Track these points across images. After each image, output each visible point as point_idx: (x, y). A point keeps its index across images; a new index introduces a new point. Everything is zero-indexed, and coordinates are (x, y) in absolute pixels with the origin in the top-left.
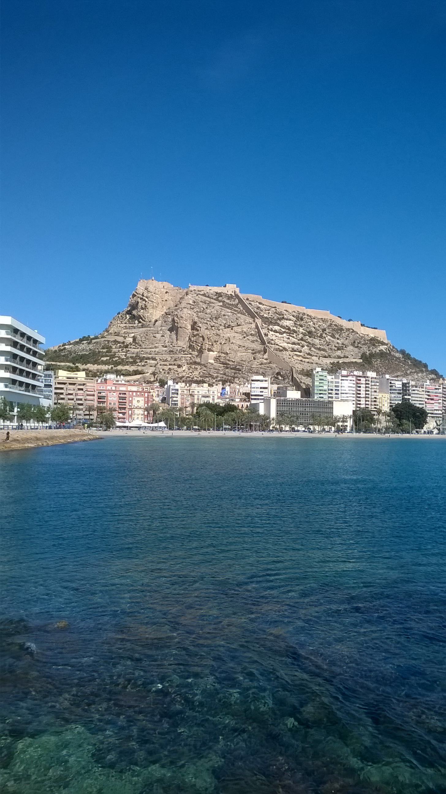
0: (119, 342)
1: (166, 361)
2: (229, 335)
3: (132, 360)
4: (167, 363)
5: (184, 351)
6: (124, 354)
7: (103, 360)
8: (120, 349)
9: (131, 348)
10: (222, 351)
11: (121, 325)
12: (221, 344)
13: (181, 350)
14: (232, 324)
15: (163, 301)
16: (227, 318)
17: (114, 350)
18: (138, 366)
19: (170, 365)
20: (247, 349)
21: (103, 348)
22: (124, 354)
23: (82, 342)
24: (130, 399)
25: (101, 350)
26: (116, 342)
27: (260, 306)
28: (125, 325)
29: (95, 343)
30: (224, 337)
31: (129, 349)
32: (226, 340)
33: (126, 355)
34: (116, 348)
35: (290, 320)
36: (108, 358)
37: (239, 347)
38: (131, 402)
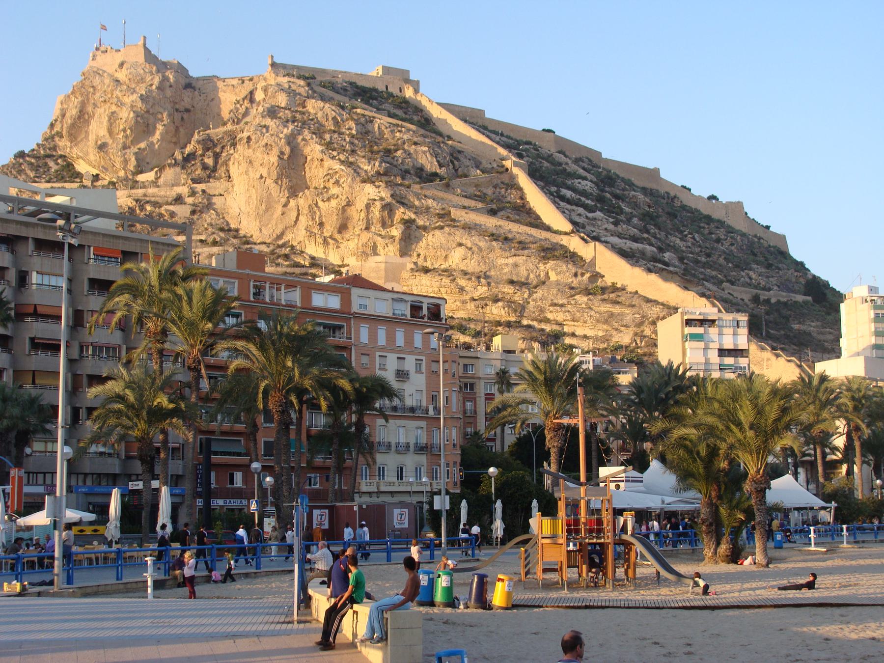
5: (286, 257)
13: (273, 253)
14: (442, 171)
16: (424, 152)
28: (49, 185)
35: (585, 178)
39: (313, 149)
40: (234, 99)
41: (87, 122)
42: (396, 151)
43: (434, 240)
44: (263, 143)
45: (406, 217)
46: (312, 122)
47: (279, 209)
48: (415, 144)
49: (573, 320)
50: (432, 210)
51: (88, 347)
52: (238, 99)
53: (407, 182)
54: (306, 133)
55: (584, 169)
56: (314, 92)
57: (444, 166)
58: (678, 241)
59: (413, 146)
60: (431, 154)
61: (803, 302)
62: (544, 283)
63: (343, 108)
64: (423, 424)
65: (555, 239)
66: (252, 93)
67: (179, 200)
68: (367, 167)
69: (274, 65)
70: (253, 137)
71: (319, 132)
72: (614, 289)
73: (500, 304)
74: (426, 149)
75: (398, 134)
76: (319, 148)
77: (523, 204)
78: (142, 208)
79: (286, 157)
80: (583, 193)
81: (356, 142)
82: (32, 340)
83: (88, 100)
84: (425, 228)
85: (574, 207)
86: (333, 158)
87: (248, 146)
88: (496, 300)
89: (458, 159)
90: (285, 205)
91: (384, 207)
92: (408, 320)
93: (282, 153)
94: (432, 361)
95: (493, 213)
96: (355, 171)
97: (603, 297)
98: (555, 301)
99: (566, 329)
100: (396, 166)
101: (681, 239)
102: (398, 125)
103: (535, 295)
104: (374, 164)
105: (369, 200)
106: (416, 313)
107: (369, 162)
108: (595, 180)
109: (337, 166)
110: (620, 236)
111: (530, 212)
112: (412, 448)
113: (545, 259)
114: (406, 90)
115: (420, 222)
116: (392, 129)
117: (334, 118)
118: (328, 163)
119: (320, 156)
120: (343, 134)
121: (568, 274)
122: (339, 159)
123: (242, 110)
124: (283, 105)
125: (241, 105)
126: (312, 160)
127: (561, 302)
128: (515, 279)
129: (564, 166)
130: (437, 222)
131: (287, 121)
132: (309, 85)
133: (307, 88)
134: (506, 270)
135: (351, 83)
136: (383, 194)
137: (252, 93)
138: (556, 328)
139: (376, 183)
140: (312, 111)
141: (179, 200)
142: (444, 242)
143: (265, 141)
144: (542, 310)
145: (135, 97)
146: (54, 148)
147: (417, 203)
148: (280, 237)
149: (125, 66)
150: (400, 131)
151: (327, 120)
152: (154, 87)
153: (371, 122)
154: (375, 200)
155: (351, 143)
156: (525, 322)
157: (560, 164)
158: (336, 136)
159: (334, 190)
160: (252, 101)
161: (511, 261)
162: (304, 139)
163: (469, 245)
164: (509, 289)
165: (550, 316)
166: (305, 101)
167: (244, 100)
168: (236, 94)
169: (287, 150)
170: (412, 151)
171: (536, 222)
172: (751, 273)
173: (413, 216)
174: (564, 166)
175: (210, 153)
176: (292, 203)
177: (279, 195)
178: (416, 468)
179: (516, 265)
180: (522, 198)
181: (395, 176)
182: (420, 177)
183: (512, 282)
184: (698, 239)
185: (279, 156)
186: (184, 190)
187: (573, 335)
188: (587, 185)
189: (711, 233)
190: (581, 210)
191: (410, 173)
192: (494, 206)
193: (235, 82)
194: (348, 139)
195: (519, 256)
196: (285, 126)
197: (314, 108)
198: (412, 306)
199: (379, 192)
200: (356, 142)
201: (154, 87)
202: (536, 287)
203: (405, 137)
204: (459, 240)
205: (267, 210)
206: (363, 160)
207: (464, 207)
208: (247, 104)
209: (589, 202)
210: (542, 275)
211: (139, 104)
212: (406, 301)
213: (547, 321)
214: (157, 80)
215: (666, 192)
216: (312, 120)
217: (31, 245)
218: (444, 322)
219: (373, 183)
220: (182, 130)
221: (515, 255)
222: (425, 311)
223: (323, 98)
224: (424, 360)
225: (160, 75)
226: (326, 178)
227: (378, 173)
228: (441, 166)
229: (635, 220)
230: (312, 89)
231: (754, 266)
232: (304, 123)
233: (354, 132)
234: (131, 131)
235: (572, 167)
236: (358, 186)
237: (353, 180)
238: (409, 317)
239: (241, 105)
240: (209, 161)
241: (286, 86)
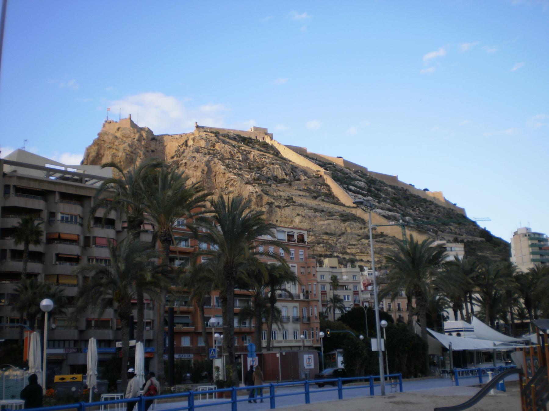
2: (288, 193)
10: (284, 219)
12: (279, 207)
14: (287, 178)
15: (148, 151)
16: (277, 168)
20: (330, 214)
32: (287, 200)
35: (360, 181)
37: (315, 212)
39: (220, 168)
40: (177, 145)
42: (263, 168)
43: (285, 213)
44: (193, 166)
45: (270, 201)
46: (219, 154)
48: (273, 164)
49: (361, 253)
50: (282, 197)
51: (93, 259)
52: (179, 145)
53: (269, 183)
54: (216, 160)
55: (359, 176)
56: (219, 139)
57: (288, 175)
58: (411, 212)
59: (272, 165)
60: (281, 169)
61: (481, 241)
62: (343, 233)
63: (234, 147)
64: (297, 304)
65: (348, 211)
66: (186, 141)
68: (249, 177)
69: (198, 127)
70: (188, 163)
71: (222, 159)
73: (322, 245)
74: (278, 166)
75: (264, 159)
76: (223, 167)
77: (330, 193)
79: (205, 172)
80: (360, 188)
81: (242, 164)
82: (57, 255)
83: (101, 147)
84: (279, 207)
85: (357, 195)
86: (230, 172)
87: (186, 167)
88: (319, 244)
89: (295, 172)
91: (258, 196)
92: (286, 243)
93: (203, 170)
94: (301, 267)
95: (315, 198)
96: (242, 178)
97: (376, 240)
98: (351, 243)
99: (358, 258)
100: (263, 176)
101: (413, 210)
102: (263, 155)
103: (340, 240)
104: (252, 175)
105: (250, 193)
106: (290, 239)
107: (249, 174)
108: (366, 181)
109: (233, 176)
110: (382, 209)
111: (334, 197)
112: (291, 319)
113: (344, 221)
114: (266, 138)
115: (276, 204)
116: (260, 157)
117: (230, 152)
118: (228, 175)
119: (223, 171)
120: (235, 160)
121: (357, 228)
122: (233, 173)
123: (182, 150)
124: (203, 146)
125: (181, 148)
126: (219, 173)
127: (354, 243)
128: (329, 232)
129: (349, 175)
130: (286, 204)
131: (206, 154)
132: (216, 136)
133: (215, 138)
134: (324, 227)
135: (238, 135)
136: (257, 190)
137: (186, 141)
138: (352, 257)
139: (254, 184)
140: (218, 149)
142: (290, 214)
143: (194, 164)
144: (344, 248)
145: (126, 145)
147: (275, 194)
149: (120, 130)
150: (264, 158)
151: (226, 153)
152: (135, 140)
153: (249, 153)
154: (253, 193)
155: (240, 165)
156: (335, 254)
157: (347, 174)
158: (231, 161)
159: (231, 189)
160: (187, 145)
161: (326, 222)
162: (214, 163)
163: (303, 215)
164: (325, 237)
165: (348, 251)
166: (214, 144)
167: (182, 145)
168: (178, 142)
169: (206, 169)
170: (271, 168)
171: (337, 202)
172: (451, 227)
173: (273, 201)
174: (349, 175)
178: (294, 332)
179: (329, 224)
180: (329, 190)
181: (263, 180)
182: (276, 181)
183: (327, 233)
184: (421, 210)
185: (202, 172)
187: (362, 260)
188: (362, 184)
189: (427, 207)
190: (360, 196)
191: (271, 179)
192: (315, 194)
193: (177, 137)
194: (237, 162)
195: (330, 219)
196: (205, 157)
197: (219, 147)
198: (288, 235)
199: (255, 189)
200: (242, 164)
201: (135, 140)
202: (340, 236)
203: (268, 161)
204: (297, 212)
206: (246, 173)
207: (300, 196)
208: (184, 147)
209: (364, 192)
210: (343, 229)
211: (128, 148)
212: (285, 232)
213: (346, 253)
214: (137, 136)
215: (402, 188)
216: (219, 153)
217: (57, 197)
218: (306, 244)
219: (252, 184)
221: (328, 219)
222: (296, 238)
223: (224, 142)
224: (296, 267)
225: (139, 133)
226: (227, 183)
227: (254, 179)
228: (286, 175)
229: (388, 201)
230: (218, 138)
231: (452, 224)
232: (214, 155)
233: (241, 159)
234: (124, 162)
235: (353, 175)
236: (244, 186)
237: (241, 182)
238: (287, 241)
239: (181, 148)
241: (204, 137)
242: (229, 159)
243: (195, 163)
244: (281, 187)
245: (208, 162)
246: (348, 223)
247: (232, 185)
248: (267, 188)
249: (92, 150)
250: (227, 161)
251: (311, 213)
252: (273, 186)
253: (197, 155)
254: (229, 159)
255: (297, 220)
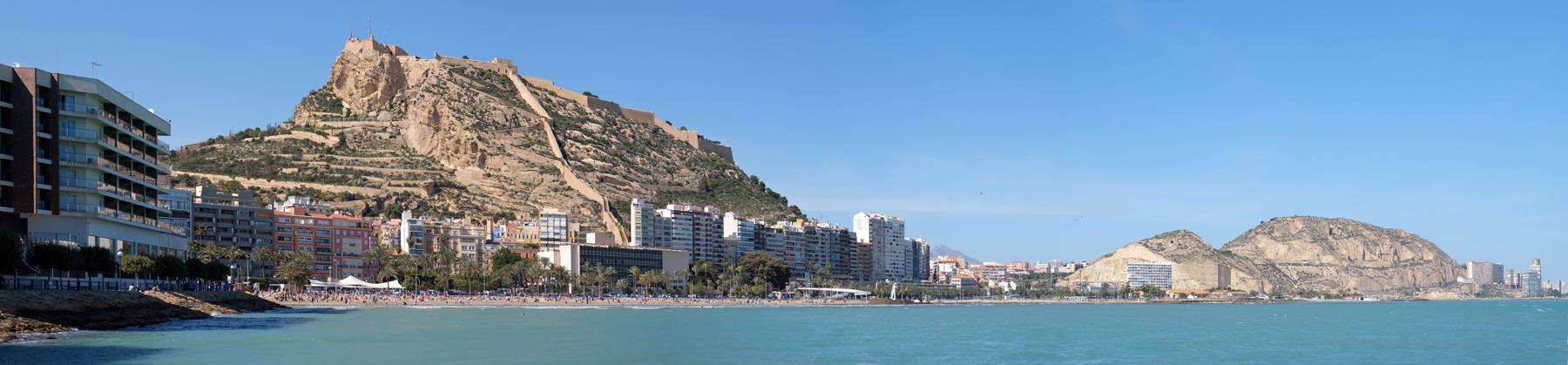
0: (315, 144)
1: (400, 177)
3: (340, 175)
4: (402, 183)
6: (325, 163)
7: (285, 174)
8: (317, 156)
9: (337, 154)
11: (317, 114)
12: (491, 155)
13: (424, 161)
17: (306, 156)
18: (350, 185)
19: (406, 185)
21: (285, 152)
22: (325, 163)
23: (246, 140)
24: (338, 241)
25: (283, 155)
26: (307, 142)
27: (553, 98)
29: (269, 141)
30: (495, 143)
31: (334, 156)
33: (328, 167)
34: (308, 152)
36: (296, 170)
37: (520, 162)
38: (340, 245)
41: (345, 79)
47: (430, 139)
54: (442, 100)
66: (427, 71)
67: (384, 130)
72: (569, 188)
78: (366, 133)
84: (491, 155)
90: (432, 137)
109: (455, 121)
115: (489, 152)
118: (452, 118)
119: (447, 114)
141: (384, 130)
146: (331, 89)
148: (430, 153)
160: (427, 76)
161: (527, 173)
164: (523, 186)
175: (403, 104)
176: (435, 137)
177: (429, 131)
183: (525, 184)
186: (387, 124)
205: (424, 139)
220: (393, 88)
227: (473, 125)
228: (507, 120)
240: (403, 109)
242: (455, 100)
243: (424, 104)
244: (497, 135)
245: (437, 102)
246: (544, 175)
247: (453, 130)
248: (483, 135)
249: (336, 69)
250: (453, 103)
251: (515, 163)
252: (490, 134)
253: (426, 94)
254: (455, 100)
255: (504, 168)
